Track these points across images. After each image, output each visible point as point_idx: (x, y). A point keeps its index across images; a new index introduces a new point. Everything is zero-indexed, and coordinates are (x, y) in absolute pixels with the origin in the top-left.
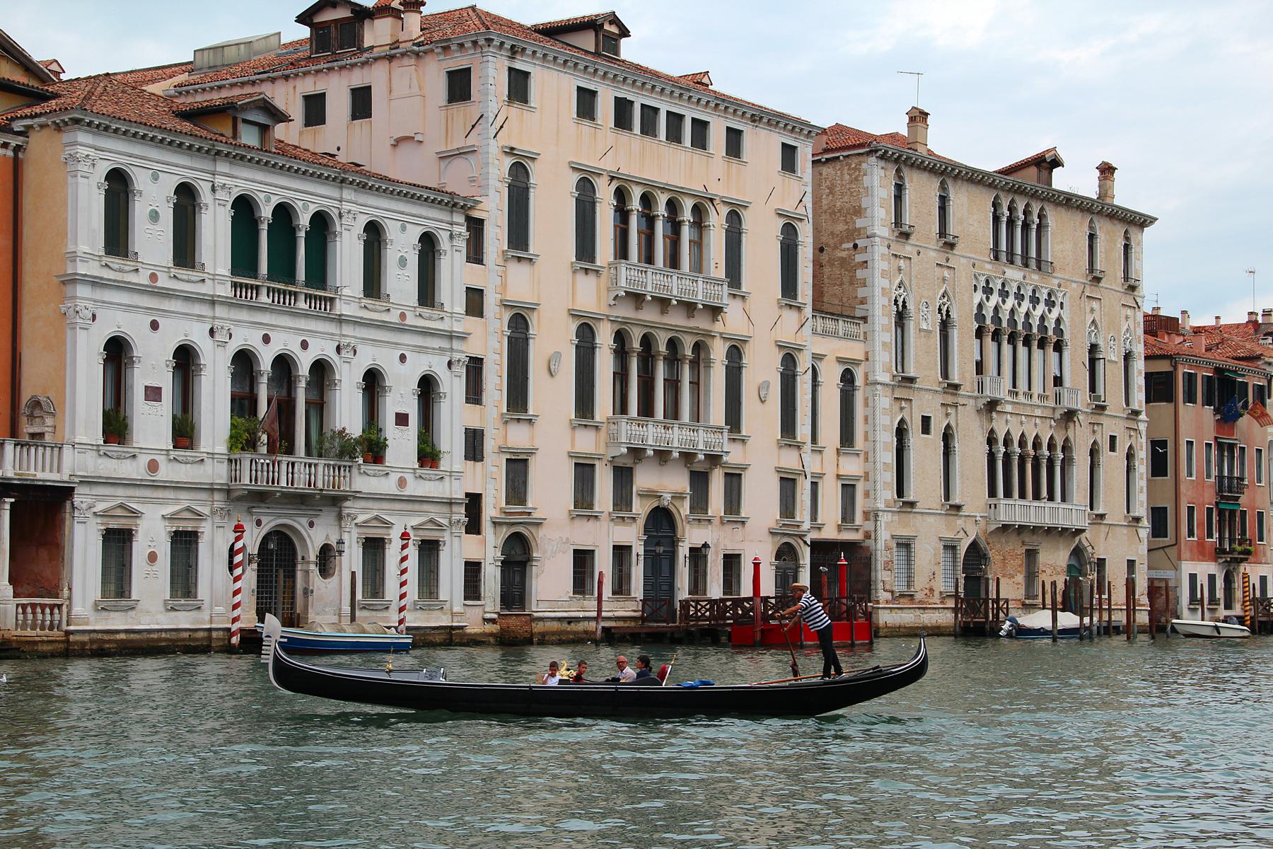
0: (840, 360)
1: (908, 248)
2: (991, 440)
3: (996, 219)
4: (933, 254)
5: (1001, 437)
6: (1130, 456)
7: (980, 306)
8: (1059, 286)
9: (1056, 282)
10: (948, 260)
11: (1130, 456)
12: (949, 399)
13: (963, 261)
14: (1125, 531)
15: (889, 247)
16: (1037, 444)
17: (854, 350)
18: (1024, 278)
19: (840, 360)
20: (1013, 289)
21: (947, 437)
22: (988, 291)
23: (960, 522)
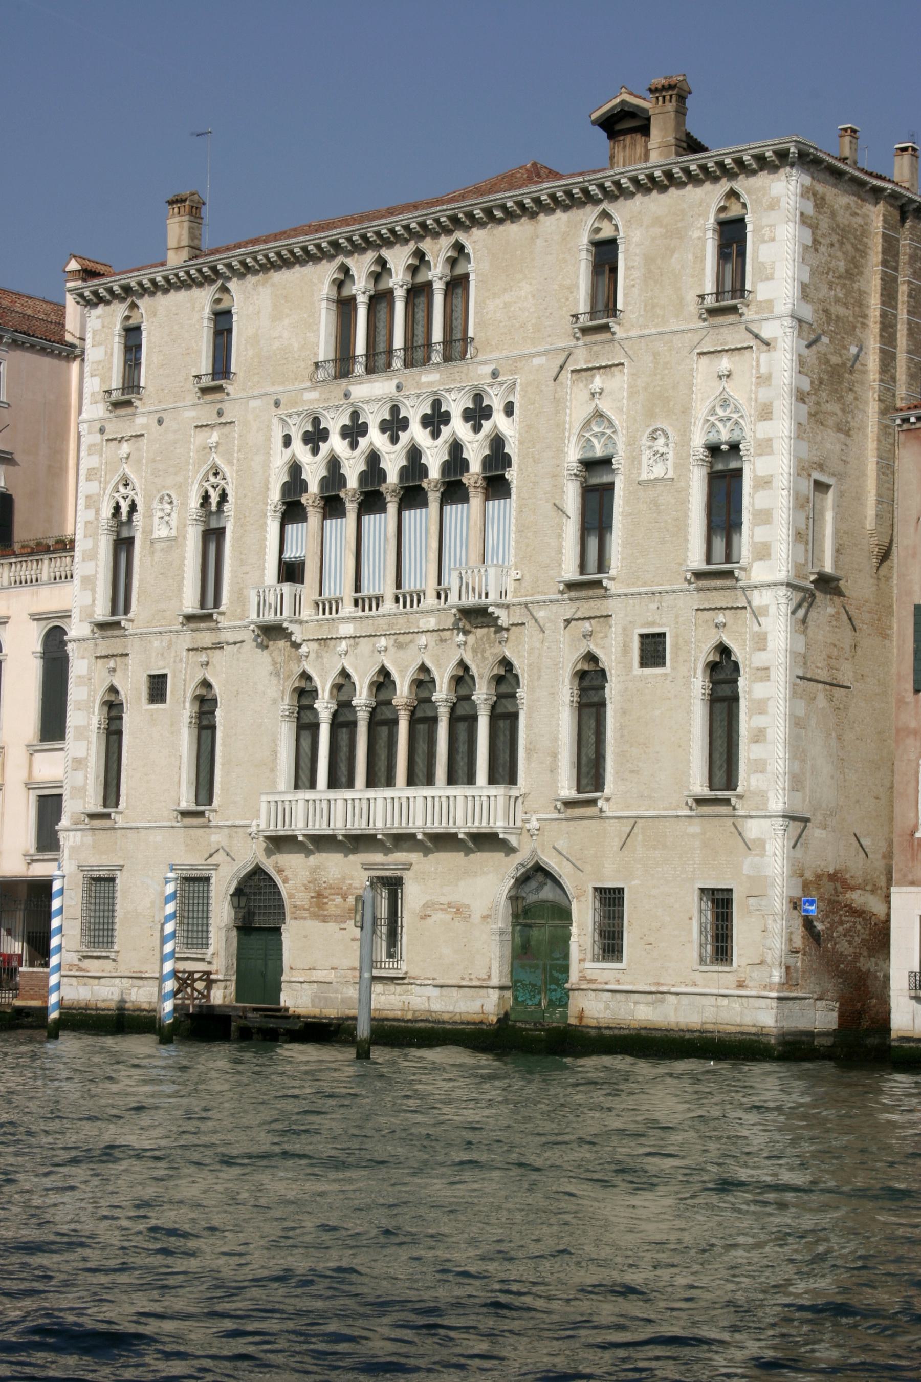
0: (37, 618)
1: (140, 420)
2: (305, 694)
3: (345, 306)
4: (190, 414)
5: (324, 685)
6: (723, 670)
7: (295, 469)
8: (495, 374)
9: (488, 369)
10: (220, 413)
11: (723, 670)
12: (206, 638)
13: (253, 404)
14: (695, 828)
15: (102, 431)
16: (423, 682)
17: (50, 599)
18: (399, 388)
19: (37, 618)
20: (373, 418)
21: (205, 705)
22: (315, 437)
23: (216, 838)
